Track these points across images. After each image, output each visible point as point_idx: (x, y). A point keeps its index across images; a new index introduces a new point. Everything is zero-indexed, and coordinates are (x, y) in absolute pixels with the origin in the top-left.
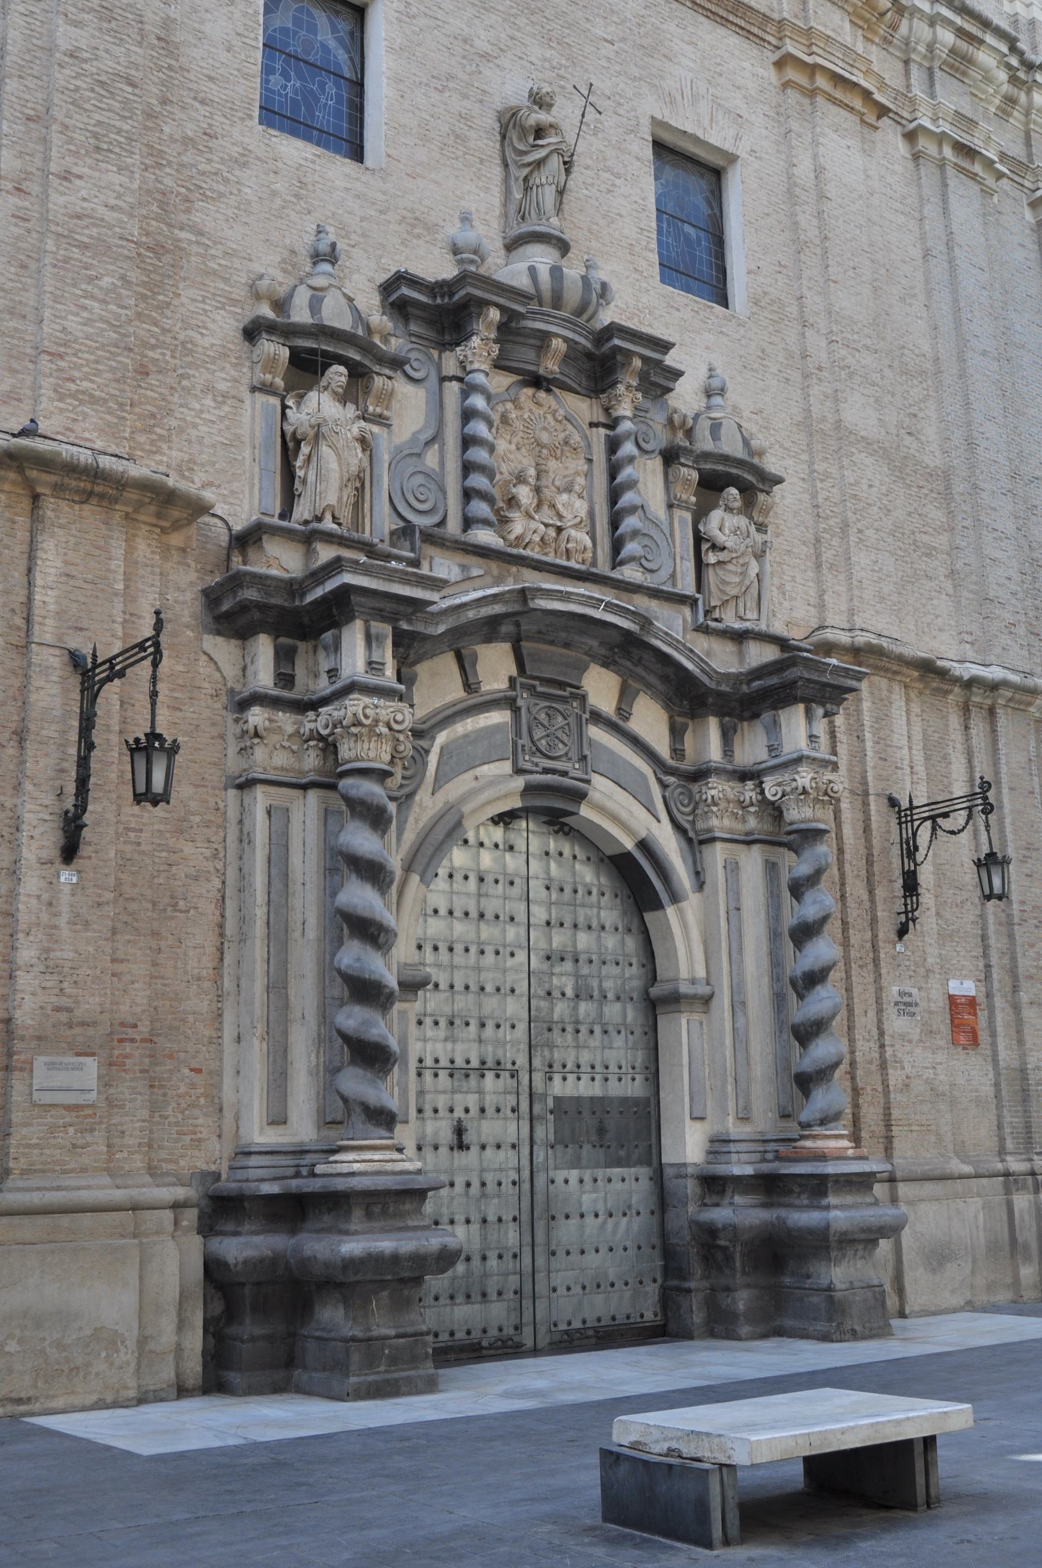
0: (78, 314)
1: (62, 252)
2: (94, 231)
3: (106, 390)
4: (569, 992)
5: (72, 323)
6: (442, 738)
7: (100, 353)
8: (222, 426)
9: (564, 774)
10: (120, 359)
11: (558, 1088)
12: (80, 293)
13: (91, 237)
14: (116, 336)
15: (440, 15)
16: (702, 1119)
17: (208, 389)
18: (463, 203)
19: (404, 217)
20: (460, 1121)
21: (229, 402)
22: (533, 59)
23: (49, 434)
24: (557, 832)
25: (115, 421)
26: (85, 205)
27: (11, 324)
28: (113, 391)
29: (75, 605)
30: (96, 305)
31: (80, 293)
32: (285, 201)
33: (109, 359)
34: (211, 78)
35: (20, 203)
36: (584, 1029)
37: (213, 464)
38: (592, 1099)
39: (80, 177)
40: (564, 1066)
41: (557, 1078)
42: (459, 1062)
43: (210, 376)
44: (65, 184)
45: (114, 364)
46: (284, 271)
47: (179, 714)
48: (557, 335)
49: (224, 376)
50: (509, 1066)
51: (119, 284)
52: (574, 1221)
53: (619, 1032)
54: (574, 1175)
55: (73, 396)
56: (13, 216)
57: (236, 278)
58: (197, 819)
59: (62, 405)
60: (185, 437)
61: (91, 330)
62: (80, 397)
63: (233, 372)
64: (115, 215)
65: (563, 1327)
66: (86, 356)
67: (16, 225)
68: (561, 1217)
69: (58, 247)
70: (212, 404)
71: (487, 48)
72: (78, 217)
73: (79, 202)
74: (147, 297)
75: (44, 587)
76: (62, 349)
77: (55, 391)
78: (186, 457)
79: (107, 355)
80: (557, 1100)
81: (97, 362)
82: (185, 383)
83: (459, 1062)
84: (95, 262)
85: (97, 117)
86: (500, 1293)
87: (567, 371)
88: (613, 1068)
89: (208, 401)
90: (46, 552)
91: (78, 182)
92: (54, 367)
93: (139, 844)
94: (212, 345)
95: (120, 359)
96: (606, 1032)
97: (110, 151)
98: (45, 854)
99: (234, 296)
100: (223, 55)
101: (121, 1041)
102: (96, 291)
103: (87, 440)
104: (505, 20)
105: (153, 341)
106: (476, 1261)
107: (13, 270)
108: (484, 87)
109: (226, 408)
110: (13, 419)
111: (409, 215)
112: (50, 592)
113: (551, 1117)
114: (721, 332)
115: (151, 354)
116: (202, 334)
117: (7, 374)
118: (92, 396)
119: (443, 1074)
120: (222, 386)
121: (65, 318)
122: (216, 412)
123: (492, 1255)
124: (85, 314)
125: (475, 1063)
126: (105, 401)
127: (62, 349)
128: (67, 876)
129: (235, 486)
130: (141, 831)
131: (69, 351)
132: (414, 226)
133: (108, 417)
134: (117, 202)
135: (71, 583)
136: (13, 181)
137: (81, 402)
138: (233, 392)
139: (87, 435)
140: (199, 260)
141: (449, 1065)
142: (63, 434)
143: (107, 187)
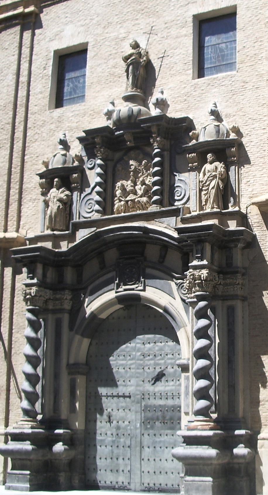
9: (133, 289)
15: (108, 35)
18: (112, 97)
19: (90, 114)
22: (142, 27)
32: (54, 131)
34: (36, 105)
71: (124, 35)
94: (32, 186)
97: (3, 146)
100: (40, 96)
104: (132, 20)
108: (123, 50)
111: (92, 112)
116: (30, 184)
120: (34, 198)
129: (36, 226)
132: (93, 115)
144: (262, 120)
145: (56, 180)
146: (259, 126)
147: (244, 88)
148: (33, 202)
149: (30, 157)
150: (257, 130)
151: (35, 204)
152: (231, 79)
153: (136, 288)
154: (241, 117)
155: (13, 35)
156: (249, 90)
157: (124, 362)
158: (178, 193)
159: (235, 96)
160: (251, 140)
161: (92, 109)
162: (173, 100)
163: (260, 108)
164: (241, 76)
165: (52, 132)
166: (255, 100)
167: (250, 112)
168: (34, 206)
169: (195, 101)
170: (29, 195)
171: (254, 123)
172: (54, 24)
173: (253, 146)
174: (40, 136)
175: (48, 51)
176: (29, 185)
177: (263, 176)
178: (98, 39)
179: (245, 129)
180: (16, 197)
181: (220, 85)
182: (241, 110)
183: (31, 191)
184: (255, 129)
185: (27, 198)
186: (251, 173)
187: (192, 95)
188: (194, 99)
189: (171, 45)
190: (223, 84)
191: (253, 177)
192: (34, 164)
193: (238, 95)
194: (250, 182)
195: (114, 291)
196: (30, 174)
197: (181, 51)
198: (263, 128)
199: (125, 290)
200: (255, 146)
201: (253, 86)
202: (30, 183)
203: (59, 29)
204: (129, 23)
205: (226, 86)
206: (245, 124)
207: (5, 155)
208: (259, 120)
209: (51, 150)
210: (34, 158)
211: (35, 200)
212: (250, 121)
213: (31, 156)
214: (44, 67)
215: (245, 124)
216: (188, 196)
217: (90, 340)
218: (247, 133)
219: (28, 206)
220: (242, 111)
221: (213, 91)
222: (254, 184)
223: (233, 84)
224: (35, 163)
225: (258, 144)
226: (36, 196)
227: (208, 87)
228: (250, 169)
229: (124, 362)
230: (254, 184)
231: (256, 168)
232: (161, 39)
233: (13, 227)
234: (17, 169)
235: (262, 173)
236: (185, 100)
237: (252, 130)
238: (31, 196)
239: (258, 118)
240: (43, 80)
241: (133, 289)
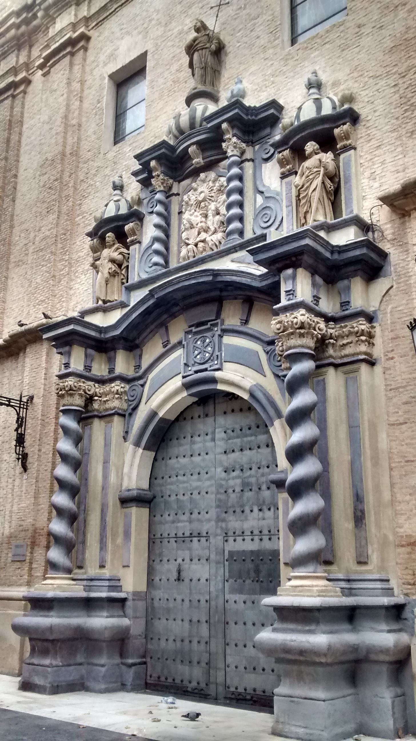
4: (238, 489)
6: (151, 376)
9: (206, 370)
11: (231, 546)
16: (128, 566)
20: (180, 565)
24: (230, 399)
32: (109, 176)
34: (89, 151)
36: (247, 509)
37: (83, 299)
38: (252, 552)
40: (234, 533)
41: (231, 539)
42: (180, 534)
48: (189, 146)
50: (205, 534)
52: (240, 626)
53: (269, 509)
54: (244, 597)
65: (232, 689)
68: (231, 623)
77: (34, 306)
80: (231, 553)
83: (180, 534)
85: (48, 201)
86: (198, 663)
87: (208, 154)
88: (266, 532)
89: (84, 276)
96: (260, 510)
101: (39, 536)
106: (187, 642)
111: (153, 138)
113: (227, 563)
114: (324, 44)
119: (172, 540)
123: (195, 641)
125: (187, 534)
126: (45, 300)
128: (25, 477)
141: (174, 536)
143: (50, 223)
144: (390, 73)
146: (386, 84)
147: (358, 36)
150: (384, 90)
151: (87, 275)
152: (338, 29)
153: (211, 366)
154: (357, 79)
155: (62, 72)
156: (367, 36)
157: (199, 483)
158: (266, 218)
159: (345, 52)
160: (375, 109)
161: (152, 134)
162: (257, 87)
163: (387, 56)
164: (354, 19)
165: (107, 178)
166: (377, 47)
167: (370, 68)
168: (86, 278)
169: (287, 79)
171: (377, 82)
172: (108, 43)
173: (378, 117)
174: (94, 187)
175: (102, 78)
177: (396, 158)
178: (159, 42)
179: (365, 94)
181: (323, 43)
182: (356, 69)
184: (380, 91)
186: (376, 159)
187: (282, 72)
188: (285, 76)
189: (250, 15)
190: (327, 40)
191: (380, 164)
193: (351, 48)
194: (376, 174)
195: (180, 377)
197: (265, 17)
198: (393, 84)
199: (196, 372)
200: (380, 117)
201: (374, 27)
203: (114, 47)
204: (196, 8)
205: (332, 42)
206: (364, 88)
208: (386, 74)
212: (371, 80)
213: (83, 216)
214: (98, 100)
215: (364, 88)
216: (281, 218)
217: (154, 454)
218: (367, 100)
219: (79, 281)
220: (358, 70)
221: (312, 55)
222: (383, 174)
223: (342, 35)
225: (386, 111)
227: (305, 54)
228: (374, 153)
229: (199, 483)
230: (383, 174)
231: (384, 149)
232: (237, 12)
235: (395, 155)
236: (273, 82)
237: (375, 93)
239: (384, 72)
240: (97, 117)
241: (206, 370)
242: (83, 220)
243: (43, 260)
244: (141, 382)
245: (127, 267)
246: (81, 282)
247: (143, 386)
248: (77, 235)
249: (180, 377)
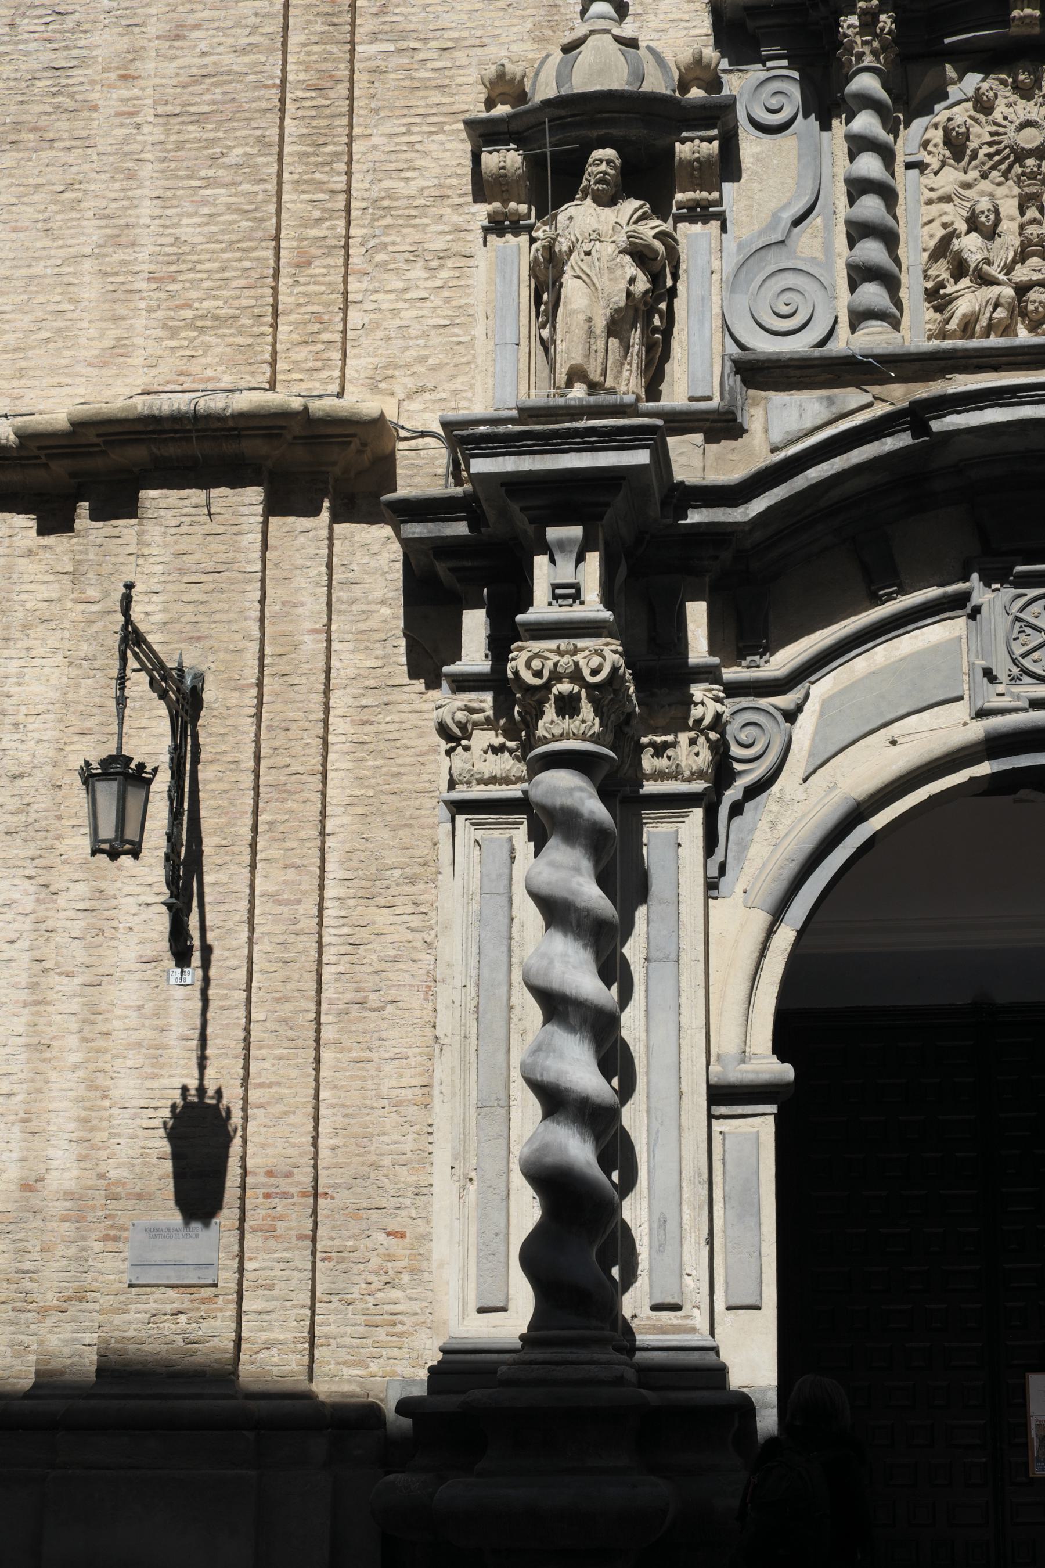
0: (195, 214)
1: (173, 138)
2: (218, 93)
3: (236, 303)
5: (189, 230)
7: (226, 256)
8: (438, 302)
10: (255, 254)
12: (198, 183)
13: (213, 102)
14: (250, 224)
17: (414, 255)
21: (450, 263)
23: (156, 388)
25: (250, 341)
26: (206, 60)
27: (116, 257)
28: (245, 302)
29: (190, 607)
30: (222, 191)
31: (198, 183)
33: (240, 260)
35: (125, 93)
39: (197, 27)
43: (414, 235)
44: (176, 44)
45: (247, 264)
46: (537, 40)
47: (369, 728)
49: (441, 228)
51: (255, 151)
55: (191, 325)
56: (118, 114)
57: (459, 80)
58: (397, 873)
59: (174, 343)
60: (380, 334)
61: (214, 229)
62: (199, 323)
63: (456, 218)
64: (247, 59)
66: (208, 266)
67: (122, 125)
69: (167, 132)
70: (424, 274)
72: (196, 83)
73: (197, 61)
74: (307, 155)
75: (146, 593)
76: (174, 268)
77: (165, 327)
78: (381, 361)
79: (238, 255)
81: (223, 269)
82: (380, 257)
84: (220, 135)
89: (418, 272)
90: (149, 545)
91: (195, 34)
92: (163, 295)
93: (295, 921)
94: (422, 189)
95: (255, 254)
98: (149, 952)
99: (457, 107)
102: (221, 172)
103: (210, 379)
105: (317, 214)
107: (117, 186)
109: (444, 274)
110: (119, 382)
112: (155, 598)
115: (313, 232)
117: (110, 324)
118: (216, 318)
120: (440, 244)
121: (178, 225)
122: (430, 284)
124: (206, 210)
126: (235, 317)
127: (174, 268)
130: (299, 902)
131: (184, 267)
133: (240, 340)
134: (251, 39)
135: (186, 579)
136: (118, 68)
137: (201, 329)
138: (456, 247)
139: (209, 373)
140: (401, 75)
142: (174, 383)
143: (237, 25)
145: (598, 153)
148: (434, 264)
149: (399, 51)
170: (405, 231)
176: (402, 184)
180: (333, 228)
183: (413, 212)
185: (393, 244)
192: (425, 86)
196: (403, 129)
202: (409, 174)
207: (256, 14)
209: (529, 25)
210: (421, 56)
211: (443, 256)
213: (404, 44)
224: (434, 83)
226: (449, 237)
233: (325, 374)
234: (332, 94)
238: (417, 236)
242: (404, 60)
243: (214, 158)
244: (785, 701)
245: (672, 293)
246: (406, 290)
247: (791, 716)
248: (377, 111)
249: (961, 711)
